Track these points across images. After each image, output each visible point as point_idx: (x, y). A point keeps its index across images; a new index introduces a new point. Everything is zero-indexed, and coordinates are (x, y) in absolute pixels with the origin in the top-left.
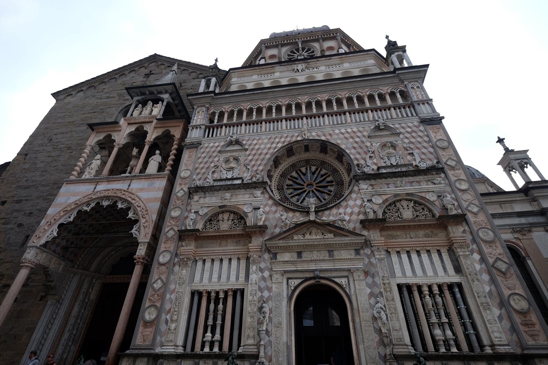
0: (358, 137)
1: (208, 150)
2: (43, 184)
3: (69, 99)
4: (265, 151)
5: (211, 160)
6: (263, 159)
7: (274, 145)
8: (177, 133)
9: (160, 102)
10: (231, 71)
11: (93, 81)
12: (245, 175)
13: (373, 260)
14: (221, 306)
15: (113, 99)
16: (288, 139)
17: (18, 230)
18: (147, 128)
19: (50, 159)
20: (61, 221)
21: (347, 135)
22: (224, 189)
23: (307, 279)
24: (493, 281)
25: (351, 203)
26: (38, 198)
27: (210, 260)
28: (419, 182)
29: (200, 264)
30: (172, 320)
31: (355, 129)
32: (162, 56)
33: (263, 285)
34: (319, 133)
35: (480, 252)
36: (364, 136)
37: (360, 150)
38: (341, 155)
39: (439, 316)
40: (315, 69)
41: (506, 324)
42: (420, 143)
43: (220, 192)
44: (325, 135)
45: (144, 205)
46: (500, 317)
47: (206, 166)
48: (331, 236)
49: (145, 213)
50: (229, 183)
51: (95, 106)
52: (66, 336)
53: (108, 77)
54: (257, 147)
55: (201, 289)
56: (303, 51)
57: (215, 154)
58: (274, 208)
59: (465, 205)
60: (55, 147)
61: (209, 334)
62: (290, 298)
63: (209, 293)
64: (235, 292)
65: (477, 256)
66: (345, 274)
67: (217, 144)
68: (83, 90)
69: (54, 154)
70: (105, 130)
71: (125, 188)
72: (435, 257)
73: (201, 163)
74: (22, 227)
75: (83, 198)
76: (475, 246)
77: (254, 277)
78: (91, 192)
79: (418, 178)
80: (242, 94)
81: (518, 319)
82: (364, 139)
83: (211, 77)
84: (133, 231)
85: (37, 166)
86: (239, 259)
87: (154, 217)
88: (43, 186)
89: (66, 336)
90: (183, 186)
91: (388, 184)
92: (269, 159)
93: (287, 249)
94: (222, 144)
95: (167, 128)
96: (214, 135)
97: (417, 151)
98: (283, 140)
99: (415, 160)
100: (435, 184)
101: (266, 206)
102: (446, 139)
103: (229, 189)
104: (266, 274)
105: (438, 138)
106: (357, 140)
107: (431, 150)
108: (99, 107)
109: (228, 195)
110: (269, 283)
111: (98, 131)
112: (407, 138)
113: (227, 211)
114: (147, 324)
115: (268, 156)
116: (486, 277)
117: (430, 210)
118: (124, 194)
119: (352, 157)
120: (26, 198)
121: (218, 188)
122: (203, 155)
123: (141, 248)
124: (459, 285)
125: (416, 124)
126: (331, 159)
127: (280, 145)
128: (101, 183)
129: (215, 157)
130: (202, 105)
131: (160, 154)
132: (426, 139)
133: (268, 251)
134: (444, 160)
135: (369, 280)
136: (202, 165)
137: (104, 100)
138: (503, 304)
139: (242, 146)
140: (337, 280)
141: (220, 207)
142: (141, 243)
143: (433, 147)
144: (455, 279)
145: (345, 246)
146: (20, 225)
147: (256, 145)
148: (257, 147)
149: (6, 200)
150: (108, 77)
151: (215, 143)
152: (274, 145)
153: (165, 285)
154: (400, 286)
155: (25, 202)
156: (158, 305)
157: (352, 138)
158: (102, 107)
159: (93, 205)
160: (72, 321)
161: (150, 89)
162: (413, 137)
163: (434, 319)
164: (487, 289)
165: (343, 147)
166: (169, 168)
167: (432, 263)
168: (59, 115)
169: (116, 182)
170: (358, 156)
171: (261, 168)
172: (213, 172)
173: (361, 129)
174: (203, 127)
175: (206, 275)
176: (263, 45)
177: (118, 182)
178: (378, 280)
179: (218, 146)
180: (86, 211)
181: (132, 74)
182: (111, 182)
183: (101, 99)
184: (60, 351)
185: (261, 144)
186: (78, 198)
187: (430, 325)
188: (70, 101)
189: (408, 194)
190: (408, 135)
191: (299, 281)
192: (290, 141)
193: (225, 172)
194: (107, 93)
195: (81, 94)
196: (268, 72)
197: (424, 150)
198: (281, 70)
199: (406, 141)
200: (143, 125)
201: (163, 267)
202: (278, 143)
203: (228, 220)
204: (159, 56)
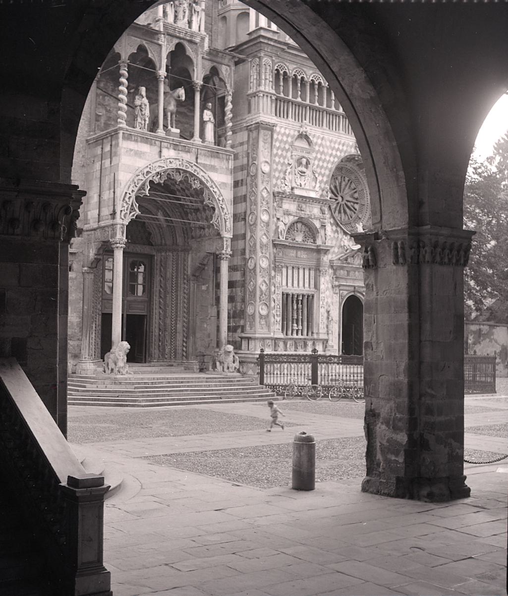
27: (291, 267)
29: (284, 270)
30: (277, 315)
45: (219, 191)
55: (290, 292)
61: (295, 325)
63: (293, 295)
64: (308, 296)
75: (153, 163)
94: (292, 133)
95: (215, 64)
141: (301, 218)
151: (286, 128)
159: (164, 178)
203: (301, 231)
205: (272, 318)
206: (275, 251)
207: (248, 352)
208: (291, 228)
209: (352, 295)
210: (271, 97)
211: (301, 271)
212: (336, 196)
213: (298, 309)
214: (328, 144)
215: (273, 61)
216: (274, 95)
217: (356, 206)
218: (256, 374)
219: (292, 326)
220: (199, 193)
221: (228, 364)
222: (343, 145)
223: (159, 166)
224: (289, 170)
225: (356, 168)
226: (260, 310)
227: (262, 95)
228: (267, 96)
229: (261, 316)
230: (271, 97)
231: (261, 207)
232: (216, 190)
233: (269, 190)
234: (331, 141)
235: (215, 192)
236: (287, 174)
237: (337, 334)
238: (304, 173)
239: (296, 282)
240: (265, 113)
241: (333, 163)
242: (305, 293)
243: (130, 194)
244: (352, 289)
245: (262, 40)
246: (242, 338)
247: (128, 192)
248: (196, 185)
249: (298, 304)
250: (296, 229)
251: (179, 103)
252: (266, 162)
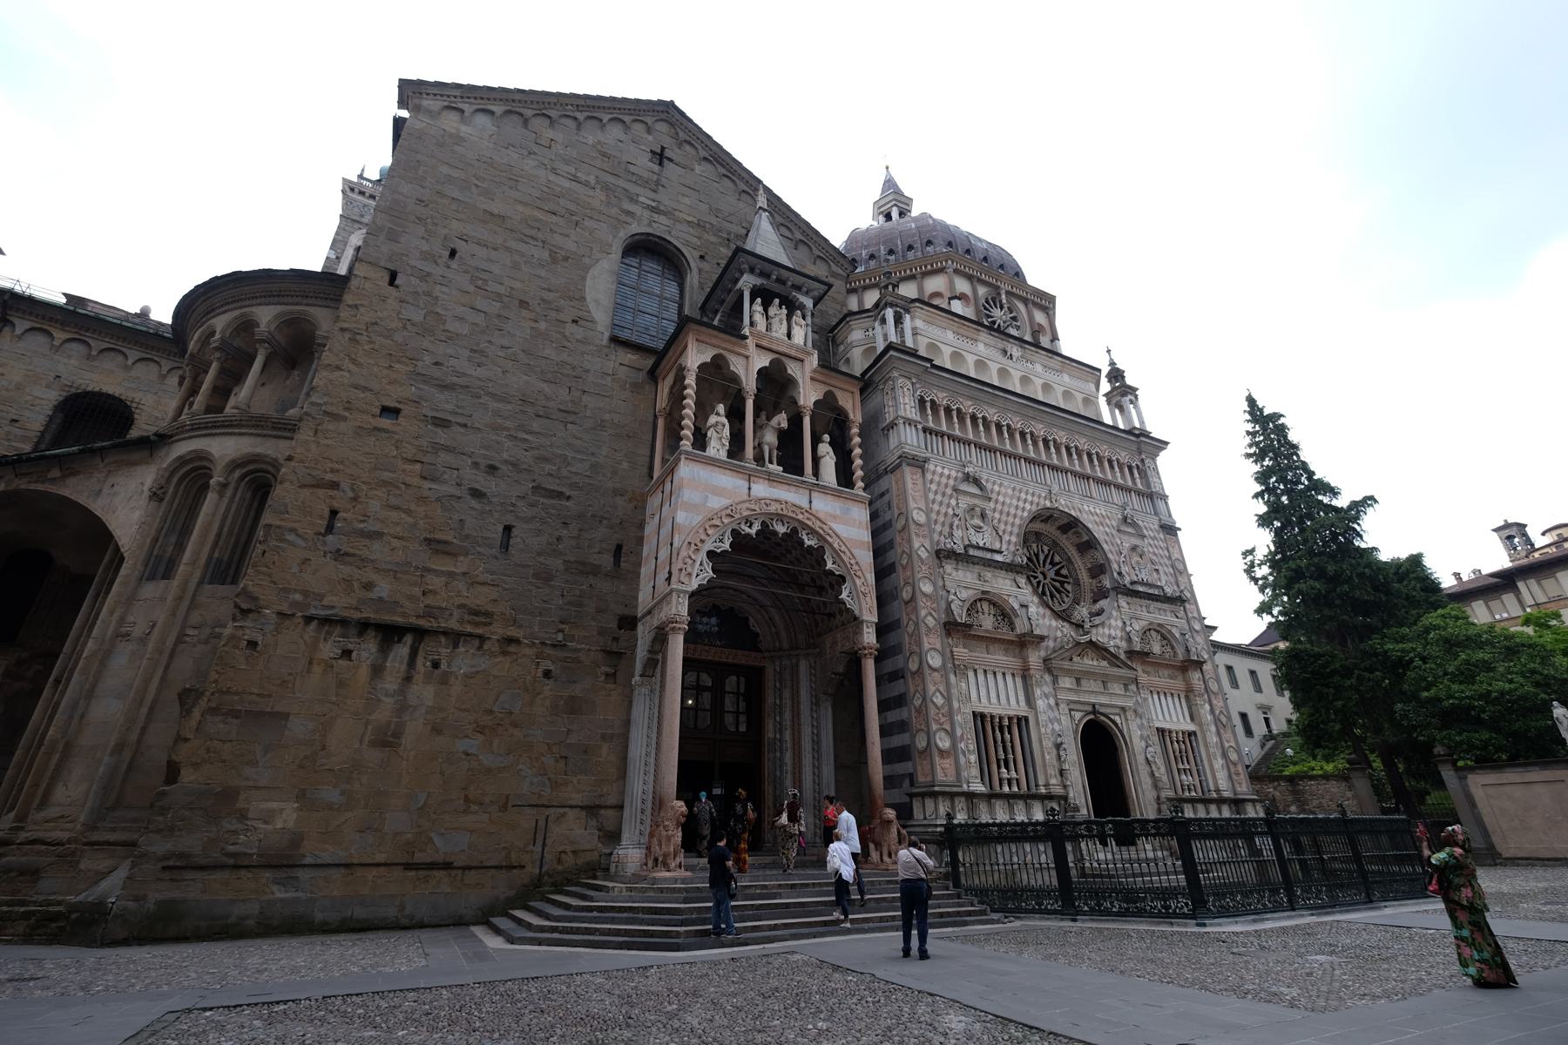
2: (490, 390)
3: (450, 122)
6: (1013, 525)
10: (917, 304)
11: (517, 97)
15: (591, 193)
17: (474, 503)
18: (792, 369)
19: (479, 319)
20: (709, 546)
22: (984, 565)
26: (496, 428)
28: (1165, 611)
29: (971, 674)
31: (1104, 513)
32: (690, 121)
34: (1069, 503)
38: (1089, 545)
40: (1029, 364)
43: (976, 566)
48: (1105, 663)
49: (857, 568)
50: (989, 556)
51: (546, 189)
53: (555, 104)
55: (986, 711)
60: (480, 283)
62: (1076, 732)
63: (992, 717)
64: (1019, 719)
66: (1117, 711)
67: (946, 472)
68: (492, 113)
69: (480, 303)
70: (714, 341)
71: (805, 505)
72: (1176, 700)
74: (485, 501)
77: (1041, 704)
78: (746, 497)
79: (1166, 606)
80: (966, 382)
83: (902, 311)
85: (447, 327)
86: (1013, 675)
88: (493, 395)
90: (921, 539)
91: (1141, 606)
93: (1069, 672)
94: (954, 474)
95: (832, 388)
96: (936, 452)
99: (1160, 580)
100: (1177, 617)
103: (990, 566)
104: (1052, 701)
108: (562, 201)
109: (988, 575)
111: (700, 338)
113: (986, 599)
115: (1018, 521)
117: (1173, 648)
118: (808, 519)
120: (461, 420)
121: (976, 560)
122: (934, 487)
123: (870, 630)
124: (1195, 733)
126: (1067, 543)
127: (1028, 506)
128: (756, 479)
129: (951, 496)
130: (906, 374)
133: (1049, 670)
137: (567, 184)
139: (981, 490)
140: (1112, 717)
141: (984, 593)
142: (867, 621)
144: (1192, 727)
145: (1117, 679)
146: (476, 494)
149: (397, 405)
150: (555, 104)
151: (943, 468)
153: (948, 698)
155: (462, 430)
156: (948, 728)
158: (573, 207)
159: (756, 527)
161: (783, 272)
166: (860, 484)
167: (1174, 704)
168: (444, 169)
169: (787, 487)
173: (1109, 515)
176: (950, 262)
177: (787, 487)
179: (949, 477)
180: (748, 535)
181: (615, 131)
182: (775, 484)
183: (554, 171)
186: (726, 502)
188: (461, 135)
189: (1159, 625)
193: (972, 531)
194: (567, 162)
195: (482, 119)
196: (964, 333)
198: (987, 341)
200: (784, 359)
201: (936, 674)
204: (682, 114)
205: (961, 756)
206: (950, 640)
207: (925, 822)
208: (973, 608)
209: (1090, 720)
210: (915, 426)
211: (999, 677)
212: (1034, 572)
213: (1003, 741)
214: (1010, 492)
215: (913, 383)
216: (920, 423)
217: (1069, 587)
218: (943, 865)
219: (999, 773)
220: (817, 555)
221: (889, 846)
222: (1033, 495)
223: (748, 509)
224: (956, 522)
225: (1058, 533)
226: (938, 741)
227: (901, 421)
228: (910, 424)
229: (942, 753)
230: (915, 426)
231: (922, 571)
232: (843, 548)
233: (928, 548)
234: (1014, 489)
235: (844, 552)
236: (955, 527)
237: (1081, 785)
238: (981, 528)
239: (993, 695)
240: (909, 439)
241: (1022, 518)
242: (1012, 713)
243: (696, 545)
244: (1090, 708)
245: (892, 353)
246: (911, 796)
247: (693, 542)
248: (809, 542)
249: (1002, 734)
250: (980, 610)
251: (782, 434)
252: (920, 509)
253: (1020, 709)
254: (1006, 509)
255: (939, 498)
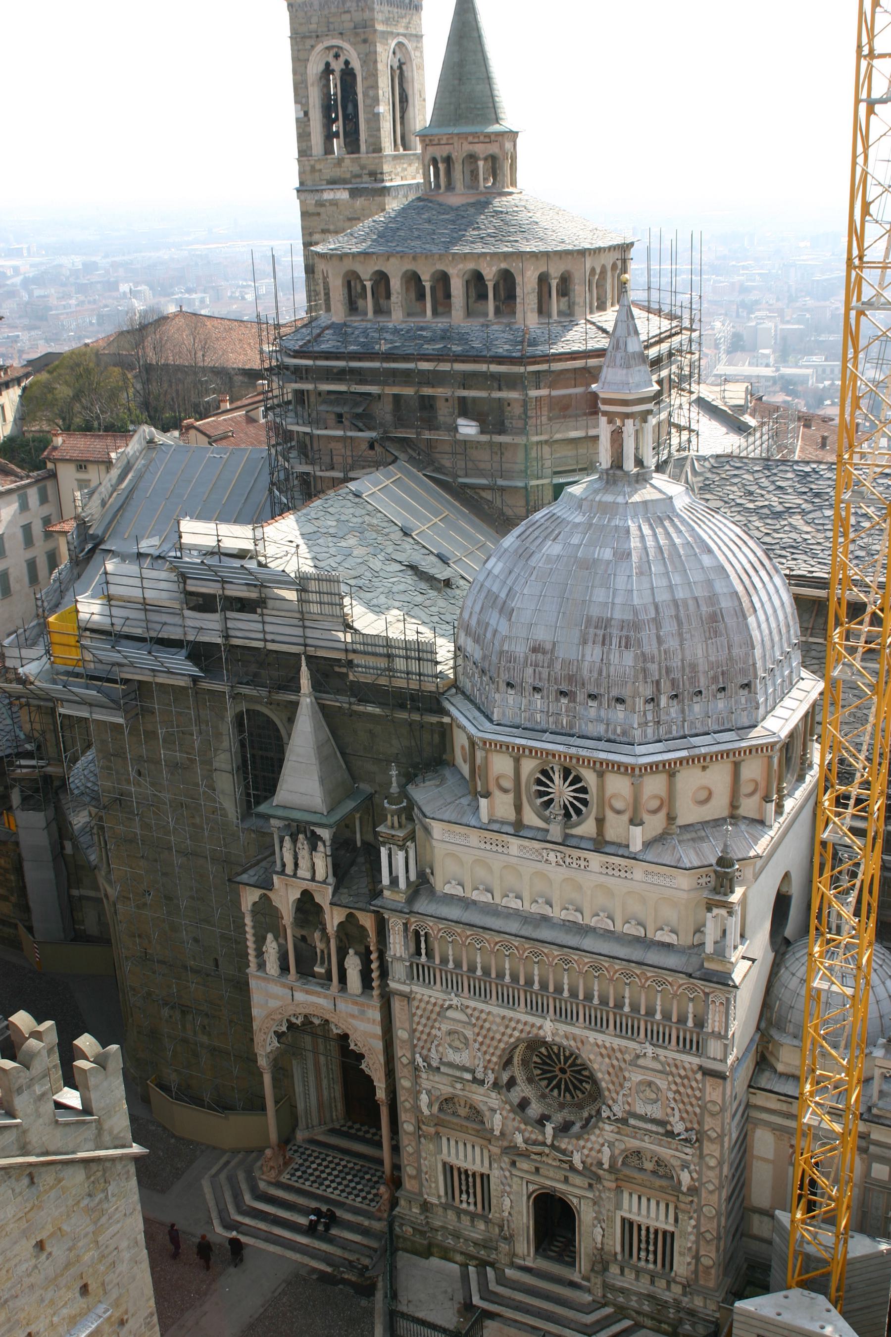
0: (617, 1059)
1: (423, 1005)
4: (498, 1036)
5: (430, 1023)
6: (496, 1048)
7: (509, 1031)
8: (367, 921)
9: (320, 843)
12: (477, 1062)
13: (603, 1195)
14: (471, 1180)
16: (528, 1028)
20: (275, 1028)
21: (603, 1051)
23: (544, 1188)
24: (697, 1242)
25: (593, 1138)
29: (444, 1140)
33: (504, 1181)
35: (698, 1220)
36: (625, 1061)
37: (615, 1079)
39: (648, 1243)
41: (692, 1267)
42: (688, 1096)
44: (575, 1040)
46: (689, 1264)
47: (427, 1030)
52: (325, 1083)
54: (487, 1025)
56: (565, 780)
57: (434, 1016)
58: (511, 1115)
59: (704, 1180)
61: (464, 1197)
62: (529, 1197)
65: (693, 1222)
73: (418, 1023)
76: (695, 1215)
81: (701, 1268)
82: (623, 1065)
84: (363, 1066)
87: (382, 1059)
89: (325, 1083)
92: (504, 1050)
94: (440, 1002)
97: (681, 1106)
98: (520, 1026)
101: (503, 1109)
102: (720, 1102)
105: (714, 1098)
106: (615, 1062)
107: (698, 1110)
110: (509, 1181)
112: (676, 1083)
114: (410, 1177)
115: (502, 1045)
116: (693, 1238)
119: (604, 1085)
122: (419, 1012)
124: (673, 1234)
125: (695, 1068)
129: (435, 1020)
131: (356, 953)
132: (698, 1093)
134: (706, 1128)
135: (596, 1208)
136: (420, 1028)
138: (697, 1258)
143: (699, 1106)
144: (670, 1228)
147: (485, 1021)
148: (487, 1025)
152: (509, 1031)
153: (418, 1152)
154: (623, 1220)
157: (609, 1057)
160: (324, 1069)
162: (684, 1085)
163: (643, 1246)
164: (689, 1245)
165: (596, 1066)
170: (611, 1087)
171: (495, 1059)
172: (437, 1046)
173: (623, 1049)
174: (408, 964)
175: (453, 1151)
178: (604, 1211)
184: (325, 1093)
185: (492, 1023)
187: (639, 1249)
190: (678, 1080)
191: (536, 1187)
192: (529, 1033)
193: (451, 1051)
197: (689, 1108)
199: (674, 1087)
202: (514, 1029)
214: (498, 1020)
241: (507, 1043)
253: (485, 1171)
254: (491, 1034)
255: (424, 1021)
